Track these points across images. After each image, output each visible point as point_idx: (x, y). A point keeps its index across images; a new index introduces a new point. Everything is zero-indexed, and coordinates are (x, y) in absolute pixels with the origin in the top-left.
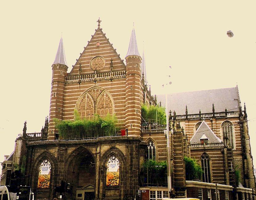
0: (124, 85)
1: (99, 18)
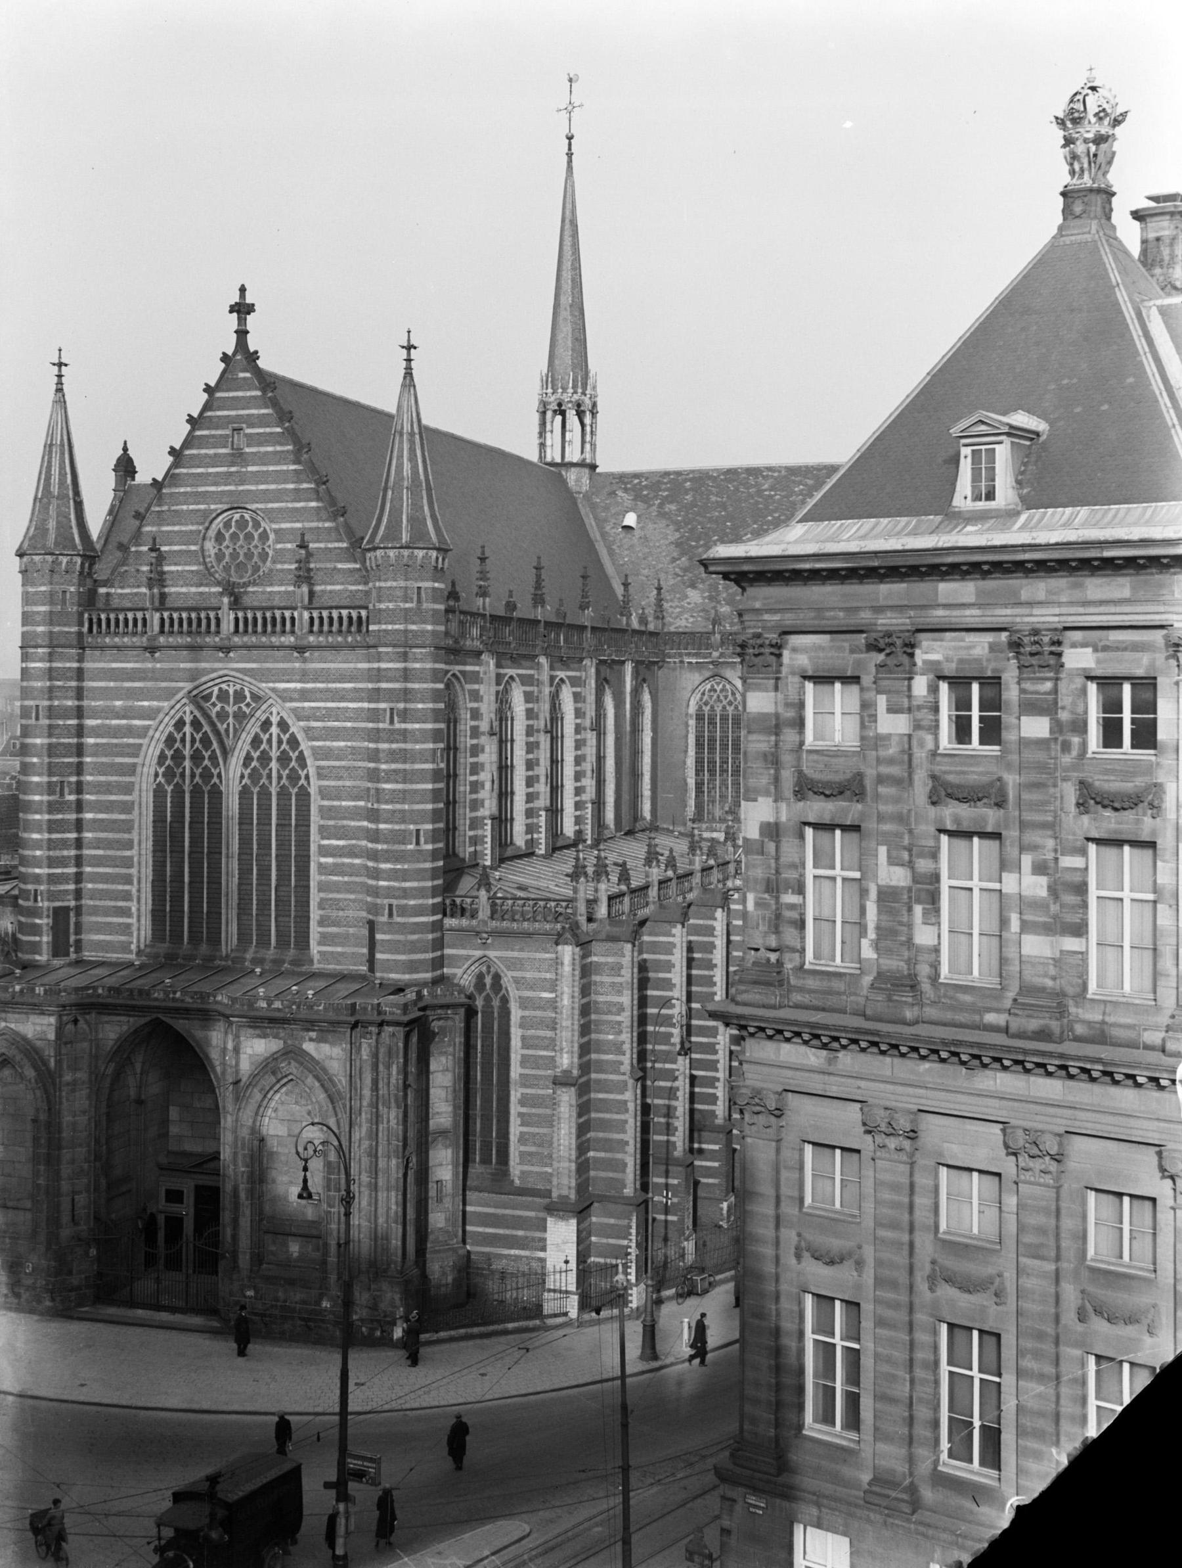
1: (243, 290)
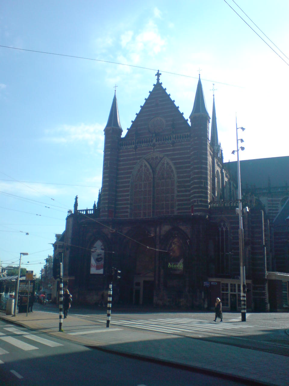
0: (188, 151)
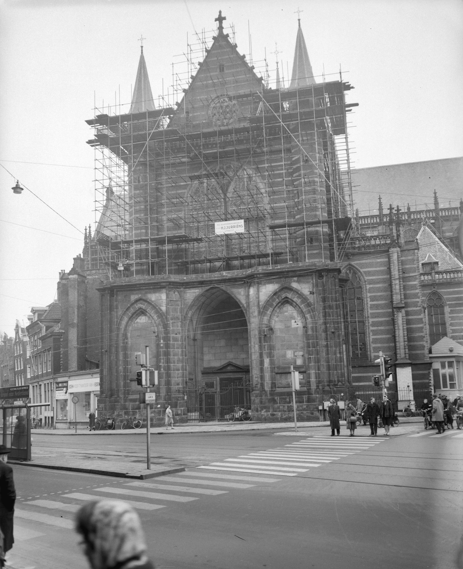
1: (220, 12)
